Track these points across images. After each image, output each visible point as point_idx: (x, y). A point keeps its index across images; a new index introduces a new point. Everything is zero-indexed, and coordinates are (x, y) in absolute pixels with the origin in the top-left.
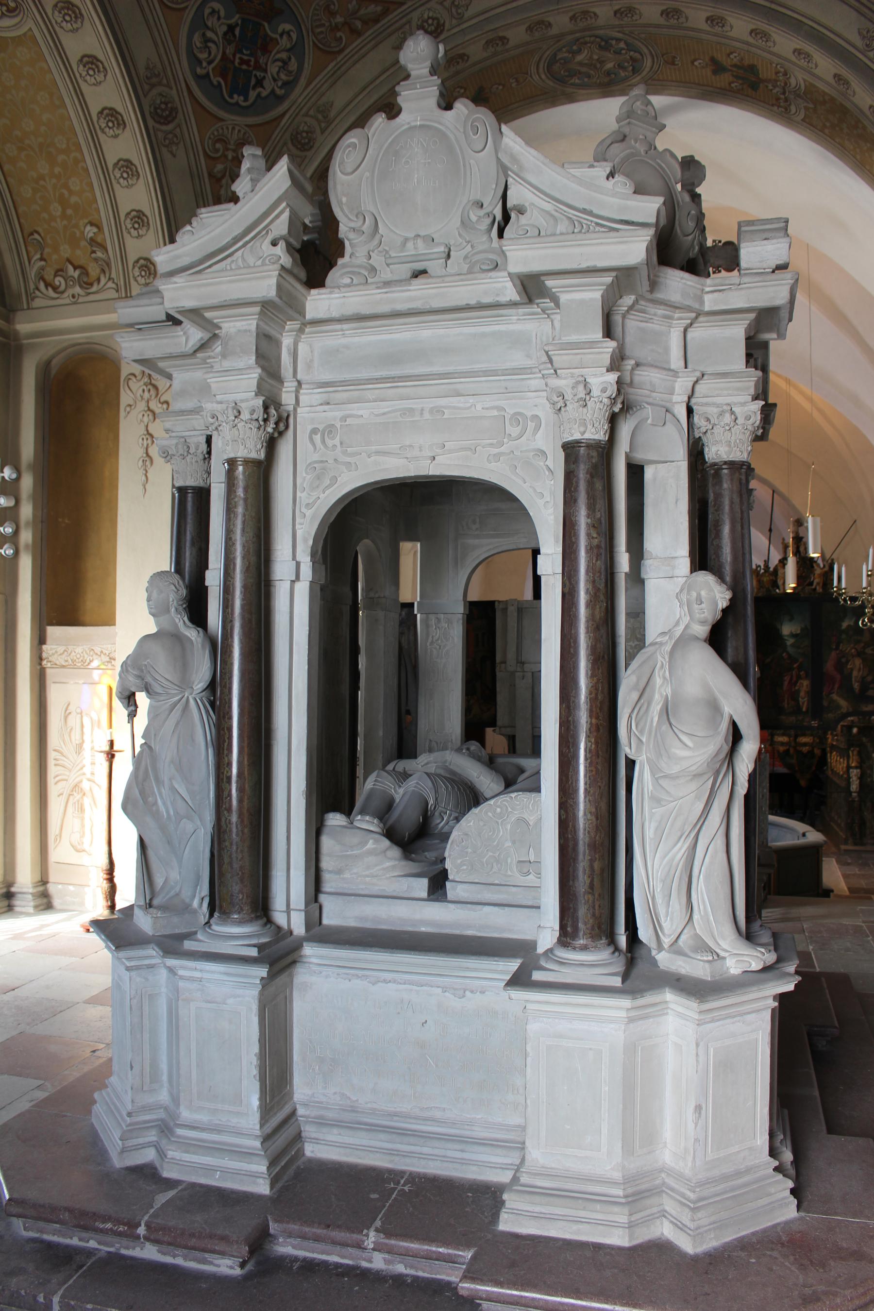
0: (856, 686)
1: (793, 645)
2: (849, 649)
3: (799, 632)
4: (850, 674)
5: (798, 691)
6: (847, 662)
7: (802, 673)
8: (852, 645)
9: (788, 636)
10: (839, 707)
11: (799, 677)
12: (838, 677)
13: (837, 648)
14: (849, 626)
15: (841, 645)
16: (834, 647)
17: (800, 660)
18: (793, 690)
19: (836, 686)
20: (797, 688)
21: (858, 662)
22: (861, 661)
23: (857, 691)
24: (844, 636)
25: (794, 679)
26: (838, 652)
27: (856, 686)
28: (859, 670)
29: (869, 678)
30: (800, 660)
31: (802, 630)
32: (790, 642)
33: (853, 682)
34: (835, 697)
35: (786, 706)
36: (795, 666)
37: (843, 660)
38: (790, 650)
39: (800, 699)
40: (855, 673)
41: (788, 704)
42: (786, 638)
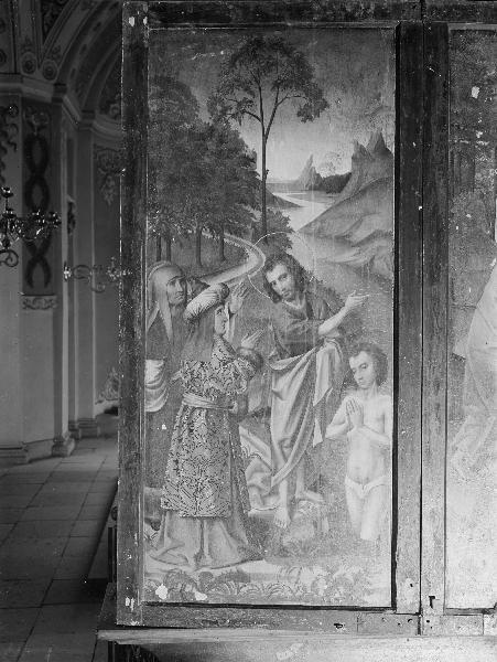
1: (317, 231)
3: (344, 168)
5: (339, 447)
7: (360, 360)
9: (293, 187)
11: (347, 381)
17: (351, 301)
18: (318, 439)
20: (333, 430)
25: (323, 387)
30: (351, 301)
31: (360, 156)
32: (305, 213)
35: (282, 514)
36: (328, 326)
38: (305, 252)
39: (349, 483)
41: (293, 504)
42: (284, 196)
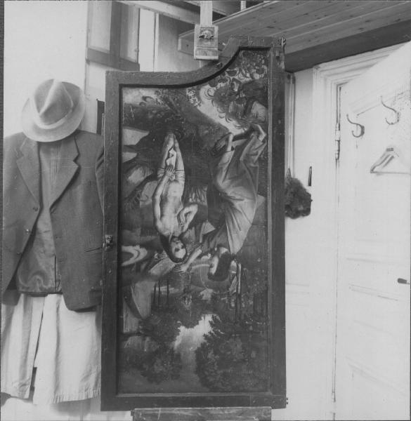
0: (173, 155)
2: (192, 259)
4: (190, 186)
6: (196, 222)
8: (184, 269)
10: (220, 99)
12: (223, 182)
13: (225, 261)
14: (191, 324)
15: (214, 271)
16: (234, 263)
19: (228, 156)
21: (168, 223)
22: (159, 225)
23: (171, 142)
24: (207, 294)
26: (224, 250)
27: (173, 155)
28: (164, 200)
29: (136, 176)
33: (181, 166)
34: (233, 128)
37: (208, 227)
40: (177, 190)
